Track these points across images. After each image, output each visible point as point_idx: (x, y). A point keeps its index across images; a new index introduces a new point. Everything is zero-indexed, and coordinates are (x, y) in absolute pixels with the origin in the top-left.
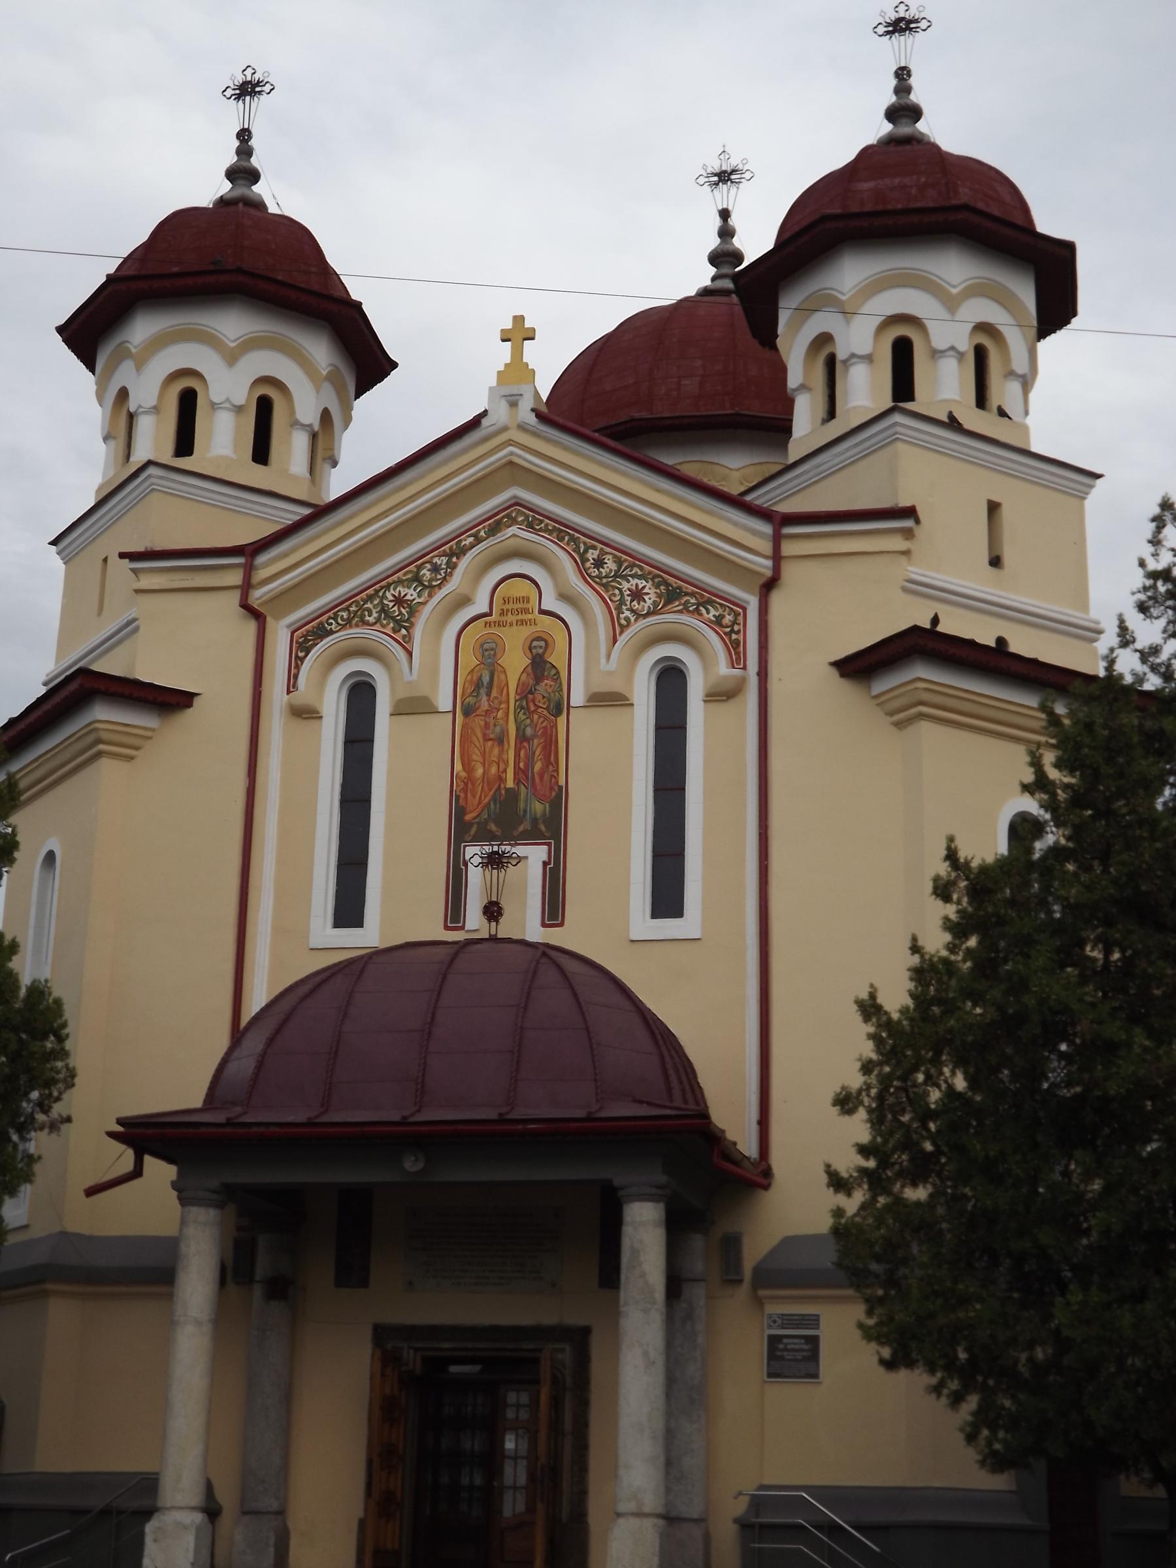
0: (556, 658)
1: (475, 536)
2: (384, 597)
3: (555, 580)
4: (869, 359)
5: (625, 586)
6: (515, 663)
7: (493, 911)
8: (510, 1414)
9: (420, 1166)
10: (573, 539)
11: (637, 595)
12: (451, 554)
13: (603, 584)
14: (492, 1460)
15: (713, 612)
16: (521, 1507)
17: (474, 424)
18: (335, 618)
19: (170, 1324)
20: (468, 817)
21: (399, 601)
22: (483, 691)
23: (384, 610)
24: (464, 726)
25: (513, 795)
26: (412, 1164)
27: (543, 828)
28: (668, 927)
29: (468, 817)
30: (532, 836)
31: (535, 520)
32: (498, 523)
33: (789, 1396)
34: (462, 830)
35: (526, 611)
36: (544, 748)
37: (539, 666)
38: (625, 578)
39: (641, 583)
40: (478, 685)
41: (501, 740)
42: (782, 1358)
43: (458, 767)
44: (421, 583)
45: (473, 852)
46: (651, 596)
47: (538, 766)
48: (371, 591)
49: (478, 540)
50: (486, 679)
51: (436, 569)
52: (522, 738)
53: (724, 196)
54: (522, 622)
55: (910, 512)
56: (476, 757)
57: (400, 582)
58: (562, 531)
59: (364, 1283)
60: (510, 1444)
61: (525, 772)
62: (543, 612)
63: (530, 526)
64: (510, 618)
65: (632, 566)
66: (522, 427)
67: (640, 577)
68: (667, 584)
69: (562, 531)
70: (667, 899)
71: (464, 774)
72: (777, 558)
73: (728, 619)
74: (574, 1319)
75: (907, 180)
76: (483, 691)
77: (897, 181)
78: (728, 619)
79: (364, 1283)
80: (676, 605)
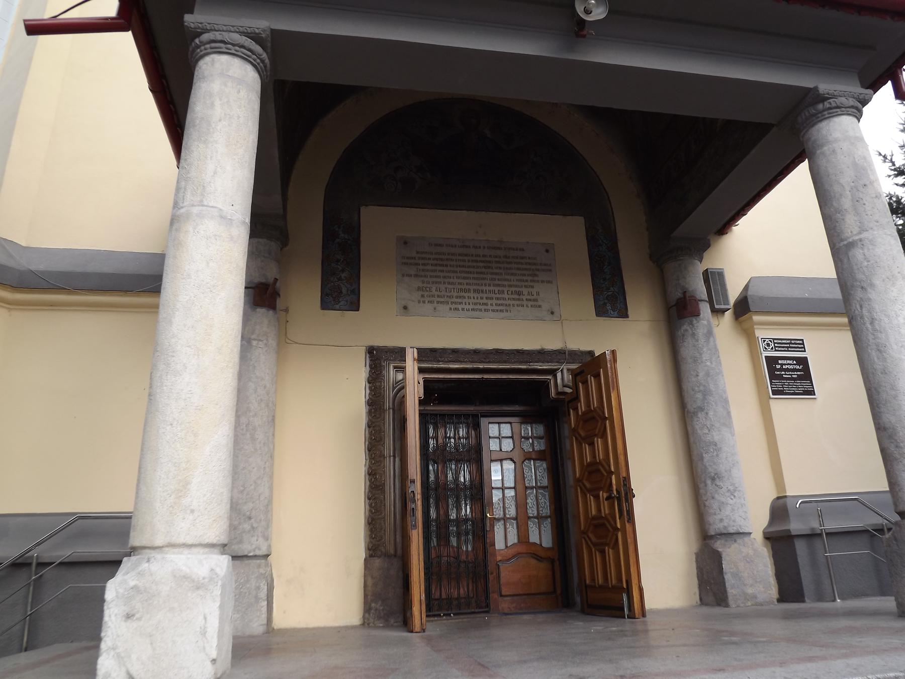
8: (494, 445)
14: (478, 490)
16: (513, 538)
33: (787, 410)
42: (780, 377)
59: (355, 306)
60: (496, 477)
74: (579, 342)
79: (355, 306)
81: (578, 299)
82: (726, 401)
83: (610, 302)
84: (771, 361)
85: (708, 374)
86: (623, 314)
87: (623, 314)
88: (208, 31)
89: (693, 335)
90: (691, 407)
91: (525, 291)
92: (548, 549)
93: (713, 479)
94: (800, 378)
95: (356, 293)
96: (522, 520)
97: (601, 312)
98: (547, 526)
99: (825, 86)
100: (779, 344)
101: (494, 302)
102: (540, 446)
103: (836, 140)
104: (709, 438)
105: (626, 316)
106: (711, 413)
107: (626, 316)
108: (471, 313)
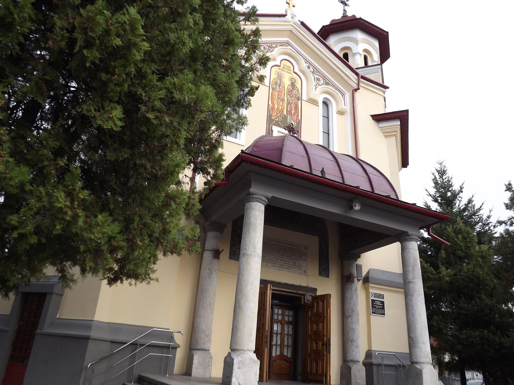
0: (298, 85)
4: (361, 55)
6: (287, 82)
17: (284, 16)
33: (375, 319)
37: (293, 85)
39: (319, 77)
40: (276, 83)
41: (283, 100)
42: (375, 307)
49: (276, 47)
50: (279, 82)
51: (265, 48)
52: (289, 103)
55: (386, 87)
56: (275, 102)
64: (285, 69)
72: (358, 85)
74: (312, 285)
81: (314, 269)
82: (358, 314)
83: (324, 272)
84: (373, 301)
85: (354, 304)
86: (328, 276)
87: (328, 276)
88: (255, 194)
89: (351, 289)
90: (347, 314)
91: (297, 262)
92: (291, 358)
93: (351, 341)
94: (381, 308)
96: (282, 346)
97: (320, 274)
98: (290, 349)
99: (410, 232)
100: (376, 295)
101: (287, 265)
102: (291, 319)
103: (411, 249)
104: (352, 327)
105: (328, 277)
106: (353, 318)
107: (328, 277)
108: (279, 268)
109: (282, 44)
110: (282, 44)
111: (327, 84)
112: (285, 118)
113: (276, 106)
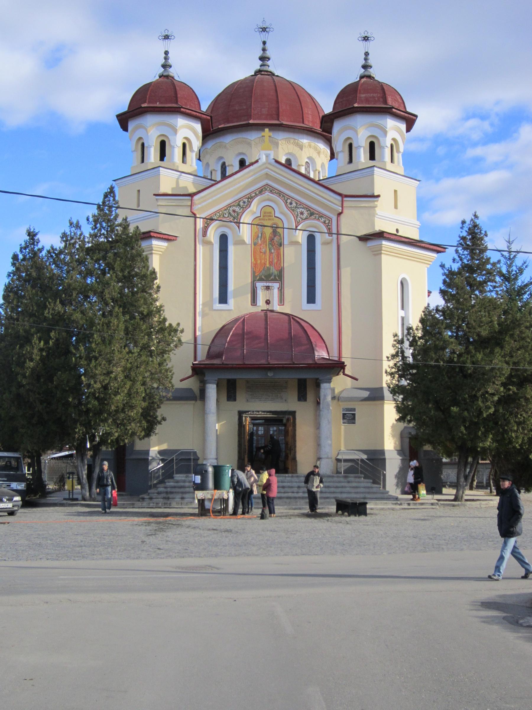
1: (255, 193)
2: (229, 210)
3: (280, 209)
5: (298, 210)
7: (268, 302)
9: (272, 374)
10: (283, 196)
11: (302, 213)
12: (248, 198)
13: (292, 210)
15: (323, 219)
18: (216, 215)
19: (203, 413)
20: (256, 274)
21: (234, 211)
22: (259, 239)
23: (229, 213)
24: (254, 248)
25: (269, 269)
26: (270, 374)
27: (277, 278)
28: (311, 306)
29: (256, 274)
30: (274, 280)
31: (273, 190)
32: (262, 190)
34: (256, 278)
35: (270, 216)
36: (277, 256)
38: (298, 208)
39: (303, 210)
43: (253, 260)
44: (240, 206)
45: (259, 285)
46: (306, 214)
47: (275, 261)
48: (226, 208)
49: (256, 195)
51: (244, 202)
53: (263, 36)
54: (270, 219)
56: (258, 257)
57: (234, 206)
58: (280, 194)
59: (235, 400)
61: (272, 262)
62: (275, 217)
63: (271, 192)
64: (266, 218)
65: (300, 205)
66: (270, 164)
67: (303, 208)
68: (310, 211)
69: (280, 194)
70: (311, 298)
71: (255, 262)
73: (327, 222)
74: (291, 409)
75: (375, 95)
76: (259, 239)
77: (372, 95)
78: (327, 222)
79: (235, 400)
80: (313, 217)
86: (305, 400)
87: (305, 400)
94: (352, 419)
95: (235, 396)
97: (299, 400)
109: (261, 191)
110: (261, 191)
111: (312, 214)
112: (269, 269)
113: (259, 262)
